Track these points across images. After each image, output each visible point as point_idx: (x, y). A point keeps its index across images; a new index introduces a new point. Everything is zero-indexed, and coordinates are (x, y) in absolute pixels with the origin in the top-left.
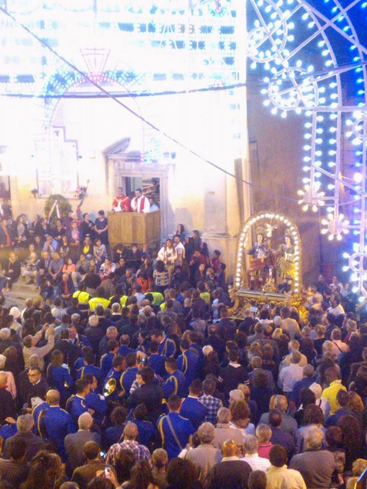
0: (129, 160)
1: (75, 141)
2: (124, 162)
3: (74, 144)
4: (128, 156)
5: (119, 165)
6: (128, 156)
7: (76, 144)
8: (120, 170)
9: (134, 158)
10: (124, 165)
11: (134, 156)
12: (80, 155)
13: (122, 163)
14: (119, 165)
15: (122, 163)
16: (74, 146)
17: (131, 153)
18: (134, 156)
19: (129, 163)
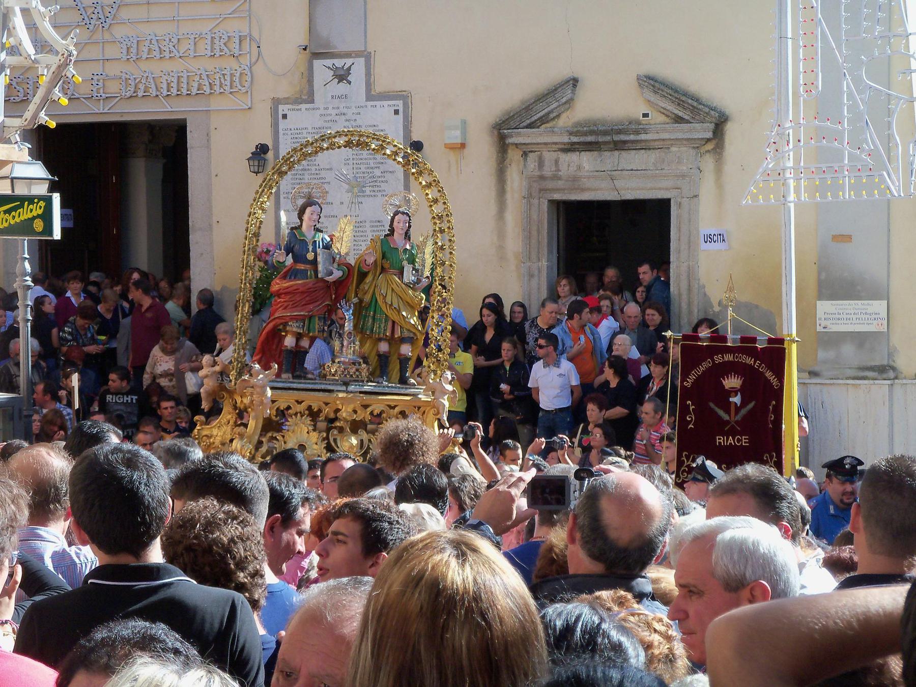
0: (570, 148)
1: (404, 97)
2: (554, 155)
3: (400, 104)
4: (571, 134)
5: (541, 163)
6: (571, 134)
7: (406, 105)
8: (542, 178)
9: (590, 139)
10: (557, 162)
11: (592, 133)
12: (415, 138)
13: (549, 156)
14: (541, 163)
15: (549, 156)
16: (396, 112)
17: (578, 124)
18: (592, 133)
19: (574, 157)
